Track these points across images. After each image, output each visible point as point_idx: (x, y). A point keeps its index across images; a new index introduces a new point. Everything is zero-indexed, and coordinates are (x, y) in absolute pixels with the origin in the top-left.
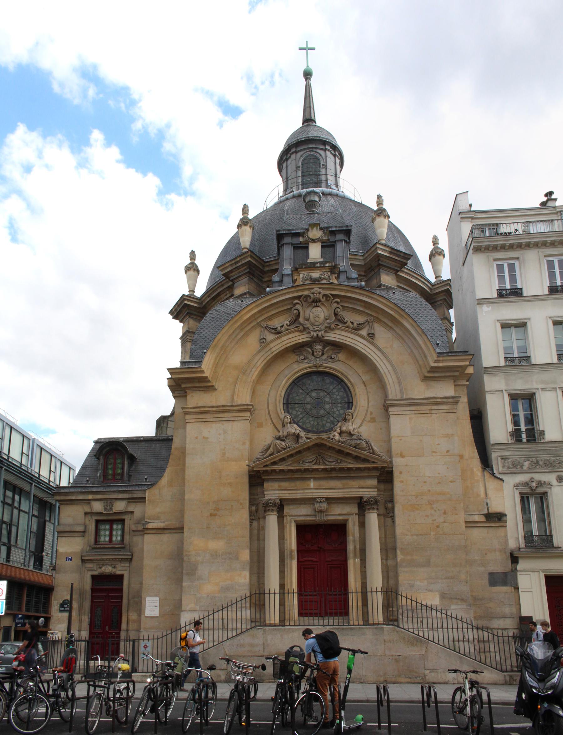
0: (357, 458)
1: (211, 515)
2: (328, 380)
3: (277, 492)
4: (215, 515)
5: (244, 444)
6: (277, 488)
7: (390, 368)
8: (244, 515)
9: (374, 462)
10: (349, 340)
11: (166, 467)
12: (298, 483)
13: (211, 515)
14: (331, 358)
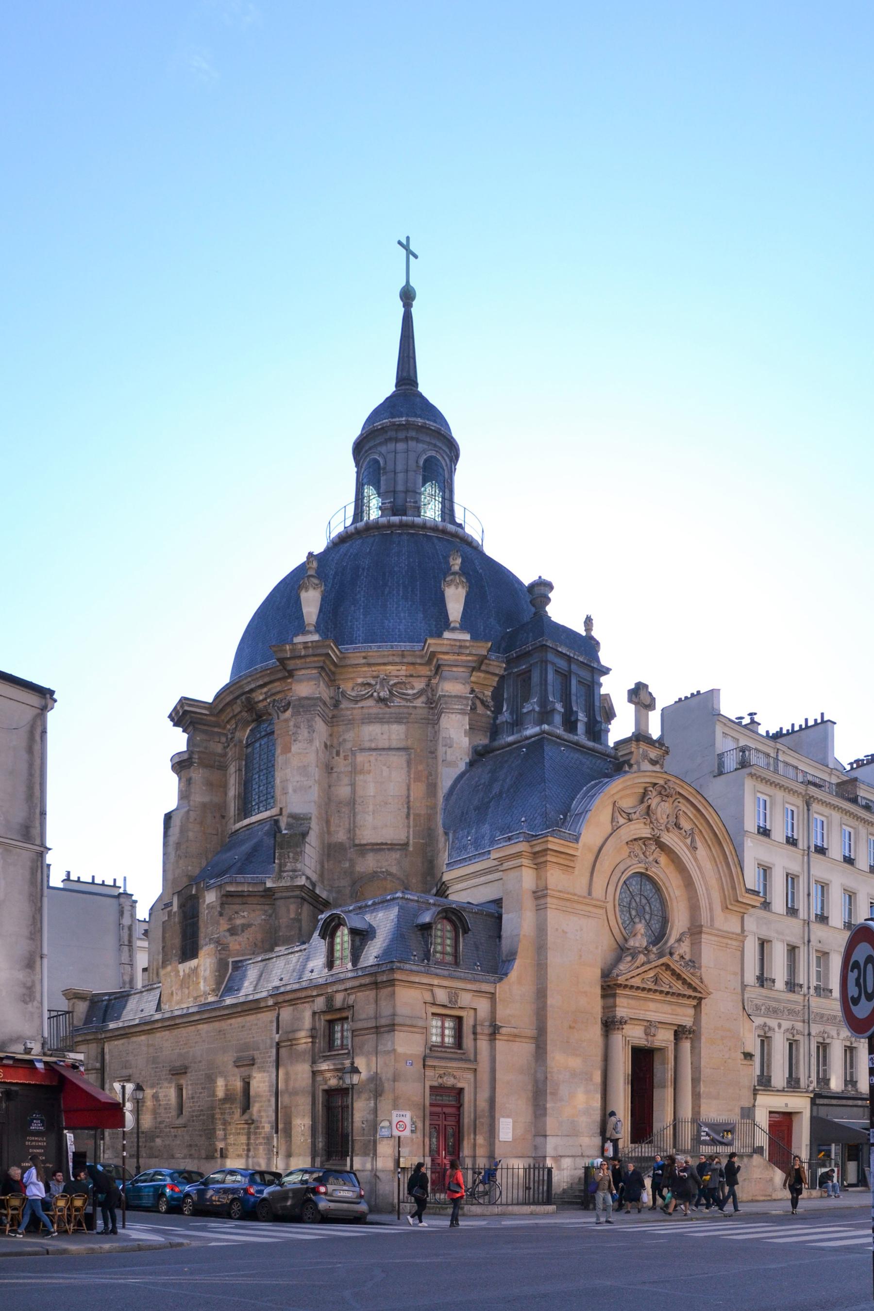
0: (690, 986)
1: (570, 1027)
2: (649, 887)
3: (625, 1010)
4: (574, 1028)
5: (597, 948)
6: (626, 1005)
7: (705, 891)
8: (596, 1030)
9: (700, 992)
10: (678, 848)
11: (515, 959)
12: (642, 1002)
13: (570, 1027)
14: (656, 862)
